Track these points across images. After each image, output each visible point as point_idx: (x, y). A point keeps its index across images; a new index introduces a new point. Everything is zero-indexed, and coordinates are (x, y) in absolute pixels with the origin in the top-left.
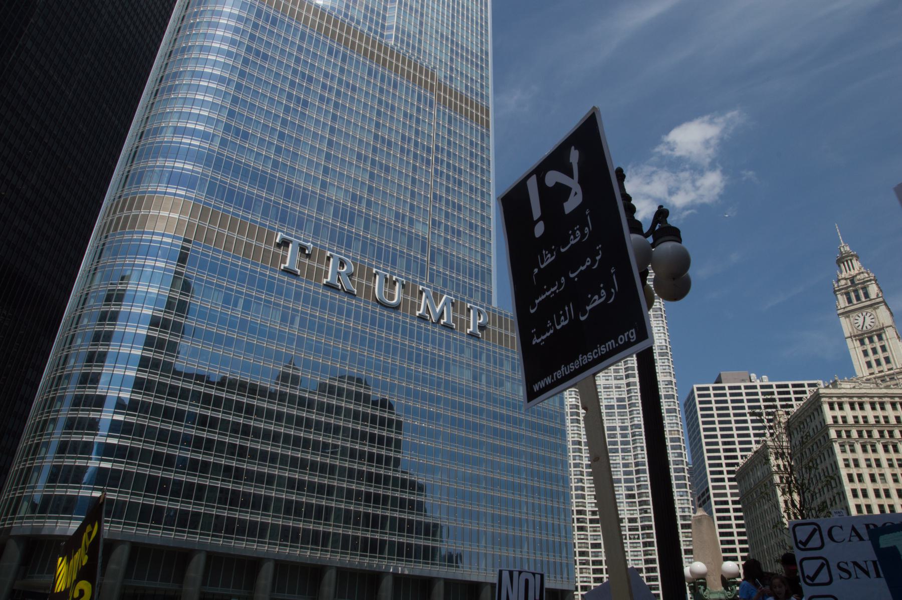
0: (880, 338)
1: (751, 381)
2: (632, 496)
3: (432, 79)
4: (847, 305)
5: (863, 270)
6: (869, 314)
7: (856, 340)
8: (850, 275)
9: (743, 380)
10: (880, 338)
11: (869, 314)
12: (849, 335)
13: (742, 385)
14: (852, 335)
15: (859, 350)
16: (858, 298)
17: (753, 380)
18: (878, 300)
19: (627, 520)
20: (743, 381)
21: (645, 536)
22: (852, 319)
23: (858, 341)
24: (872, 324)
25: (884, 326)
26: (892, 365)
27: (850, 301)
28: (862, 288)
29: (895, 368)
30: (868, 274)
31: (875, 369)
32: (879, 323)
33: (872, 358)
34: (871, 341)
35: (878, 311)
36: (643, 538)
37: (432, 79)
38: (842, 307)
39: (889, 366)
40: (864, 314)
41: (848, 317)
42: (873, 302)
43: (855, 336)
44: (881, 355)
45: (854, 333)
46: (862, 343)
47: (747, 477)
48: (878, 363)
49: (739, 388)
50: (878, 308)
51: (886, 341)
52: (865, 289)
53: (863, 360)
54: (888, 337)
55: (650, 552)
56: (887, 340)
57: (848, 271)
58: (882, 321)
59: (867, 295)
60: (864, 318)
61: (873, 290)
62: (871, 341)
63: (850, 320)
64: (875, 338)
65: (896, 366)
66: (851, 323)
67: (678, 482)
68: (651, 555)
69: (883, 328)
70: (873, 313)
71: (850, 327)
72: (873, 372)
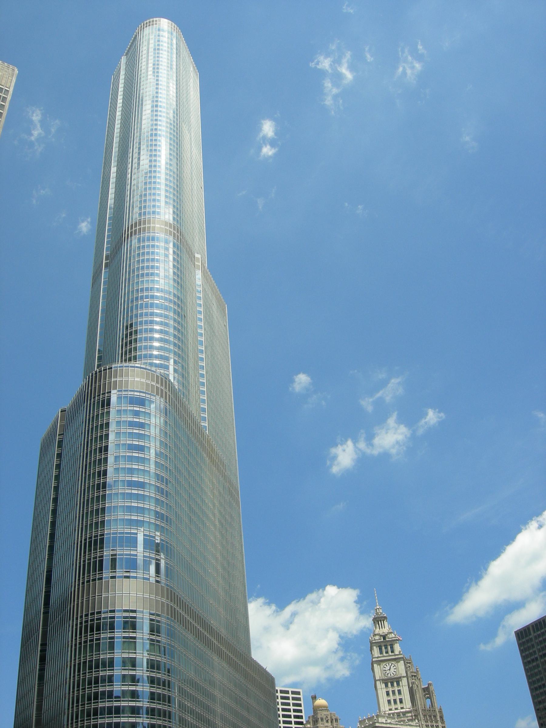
0: (398, 684)
4: (379, 655)
5: (391, 631)
6: (393, 665)
7: (383, 683)
8: (383, 633)
10: (398, 684)
11: (393, 665)
12: (379, 678)
14: (381, 678)
15: (384, 691)
16: (387, 652)
18: (400, 656)
22: (382, 667)
23: (384, 684)
24: (394, 673)
25: (402, 676)
26: (403, 705)
27: (381, 652)
28: (390, 645)
29: (405, 707)
30: (395, 635)
31: (393, 706)
32: (399, 672)
33: (392, 698)
34: (392, 685)
35: (399, 664)
38: (376, 656)
39: (402, 706)
40: (390, 664)
41: (380, 665)
42: (397, 657)
43: (382, 680)
44: (398, 697)
45: (382, 677)
46: (387, 686)
48: (395, 701)
50: (399, 662)
51: (401, 687)
52: (392, 648)
53: (386, 698)
54: (403, 684)
56: (402, 686)
57: (381, 629)
58: (401, 672)
59: (392, 652)
60: (390, 667)
61: (397, 648)
62: (392, 685)
63: (380, 667)
64: (395, 684)
65: (406, 706)
66: (381, 669)
69: (400, 677)
70: (396, 665)
71: (380, 672)
72: (391, 708)
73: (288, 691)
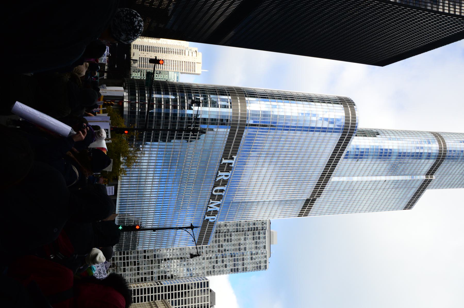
1: (210, 306)
2: (155, 257)
3: (316, 197)
9: (211, 303)
13: (209, 302)
17: (211, 307)
19: (145, 254)
20: (211, 303)
21: (138, 262)
36: (137, 261)
37: (316, 197)
47: (163, 305)
49: (208, 301)
55: (132, 264)
67: (161, 276)
68: (131, 264)
73: (208, 301)
